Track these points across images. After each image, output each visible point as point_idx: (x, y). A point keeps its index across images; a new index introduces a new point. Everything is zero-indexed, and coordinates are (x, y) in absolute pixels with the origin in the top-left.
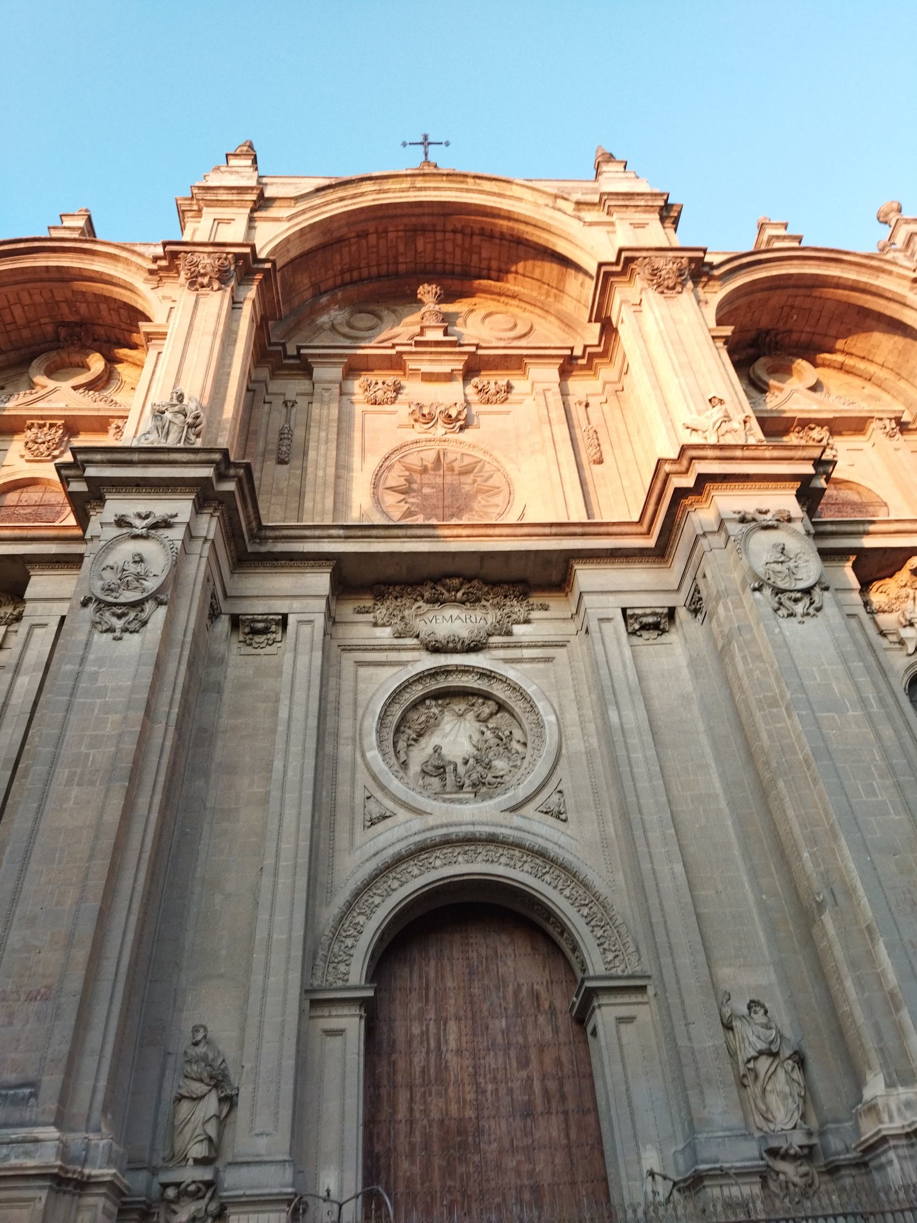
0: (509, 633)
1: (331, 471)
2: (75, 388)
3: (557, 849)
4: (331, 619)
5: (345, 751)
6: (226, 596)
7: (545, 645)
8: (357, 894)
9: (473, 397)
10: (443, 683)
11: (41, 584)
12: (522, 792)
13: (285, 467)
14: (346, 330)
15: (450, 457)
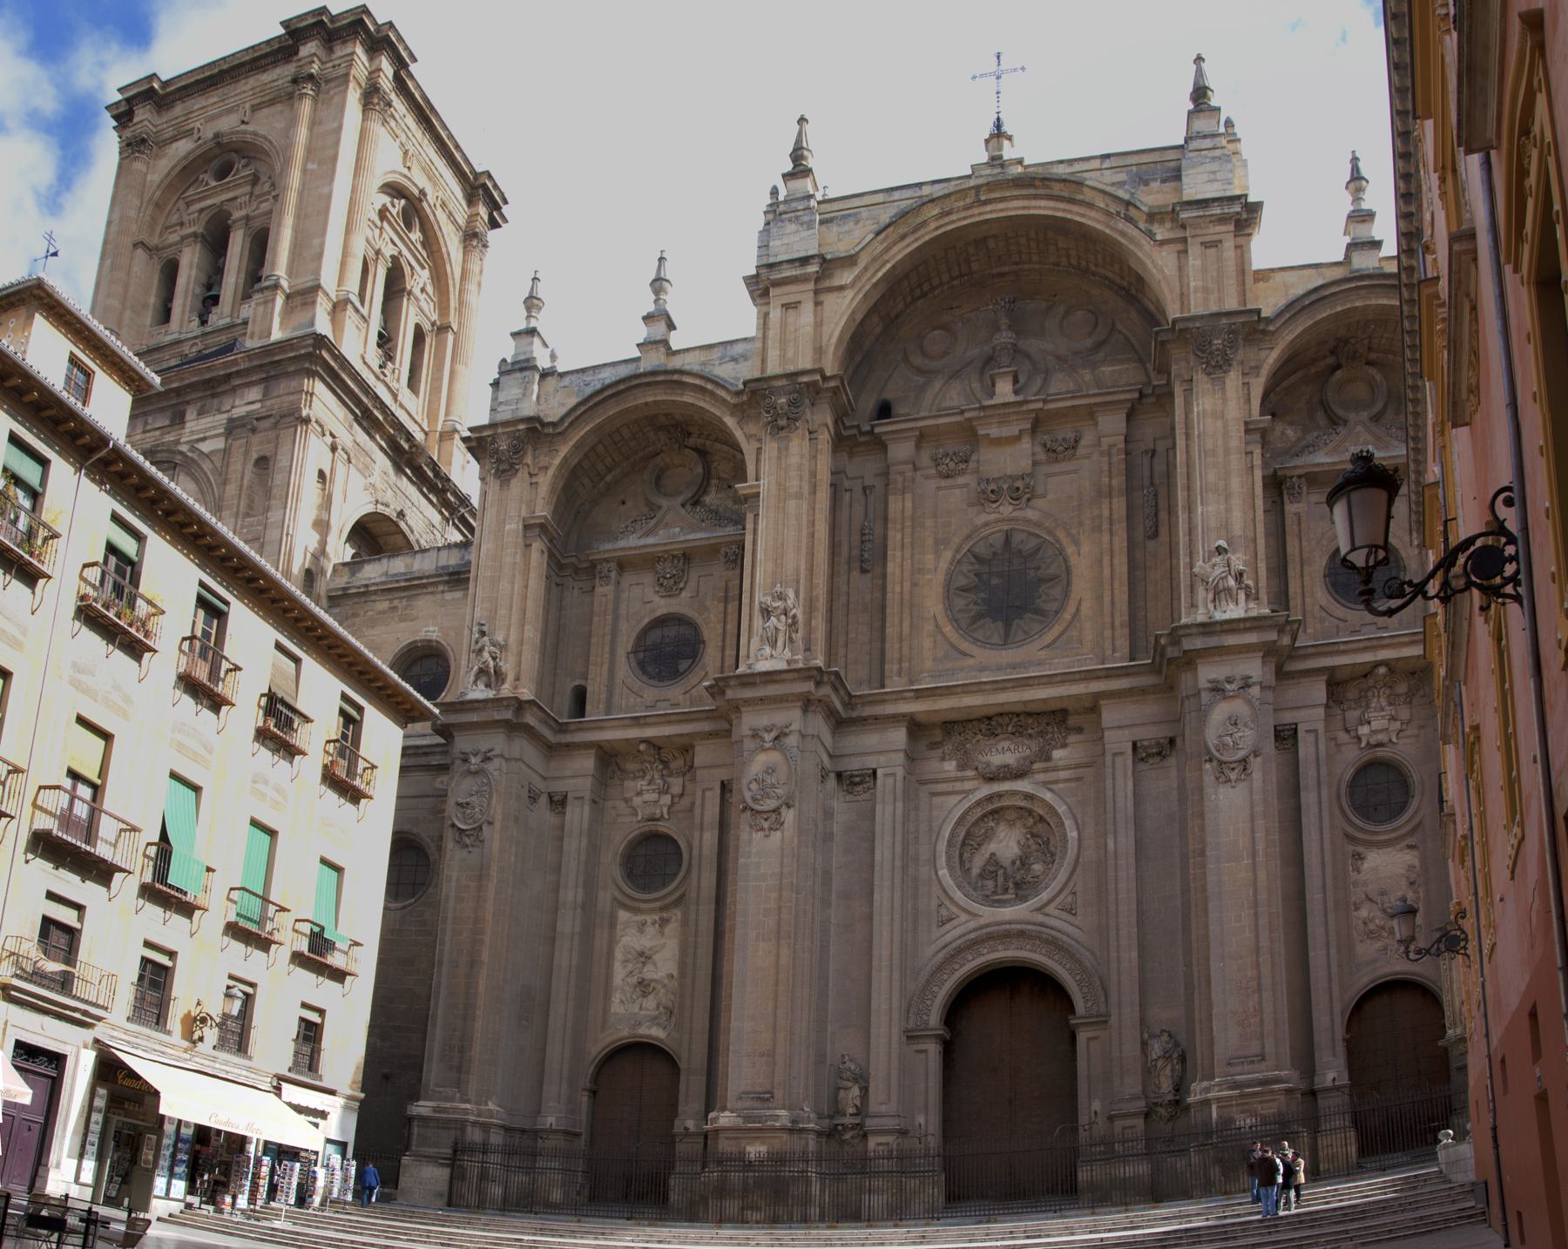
0: (1049, 759)
1: (907, 585)
2: (683, 505)
3: (1065, 938)
4: (911, 758)
5: (924, 870)
6: (831, 756)
7: (1077, 767)
8: (933, 975)
9: (1042, 456)
10: (997, 805)
11: (704, 754)
12: (1045, 896)
13: (869, 576)
14: (918, 360)
15: (1017, 539)
